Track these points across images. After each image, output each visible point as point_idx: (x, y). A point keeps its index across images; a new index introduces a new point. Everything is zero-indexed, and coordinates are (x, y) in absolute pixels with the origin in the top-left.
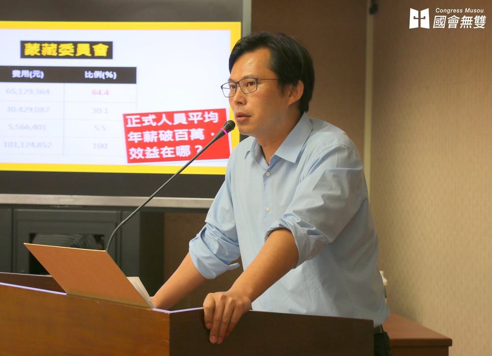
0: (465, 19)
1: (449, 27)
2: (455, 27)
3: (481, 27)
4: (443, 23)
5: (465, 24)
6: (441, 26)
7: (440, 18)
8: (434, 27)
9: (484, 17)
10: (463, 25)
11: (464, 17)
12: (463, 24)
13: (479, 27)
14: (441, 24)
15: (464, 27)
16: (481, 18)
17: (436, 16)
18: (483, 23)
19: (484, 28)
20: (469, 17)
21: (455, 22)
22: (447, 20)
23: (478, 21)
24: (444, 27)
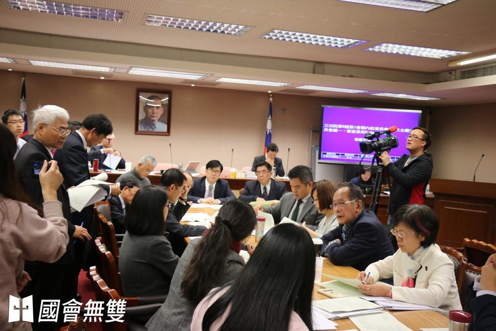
0: (91, 305)
1: (65, 321)
2: (75, 321)
3: (117, 320)
4: (55, 313)
5: (92, 314)
6: (51, 318)
7: (49, 303)
8: (40, 320)
9: (124, 302)
10: (88, 317)
11: (90, 302)
12: (88, 314)
13: (114, 320)
14: (51, 315)
15: (90, 321)
16: (118, 304)
17: (43, 301)
18: (121, 312)
19: (122, 321)
20: (97, 303)
21: (75, 311)
22: (62, 308)
23: (113, 309)
24: (56, 320)
